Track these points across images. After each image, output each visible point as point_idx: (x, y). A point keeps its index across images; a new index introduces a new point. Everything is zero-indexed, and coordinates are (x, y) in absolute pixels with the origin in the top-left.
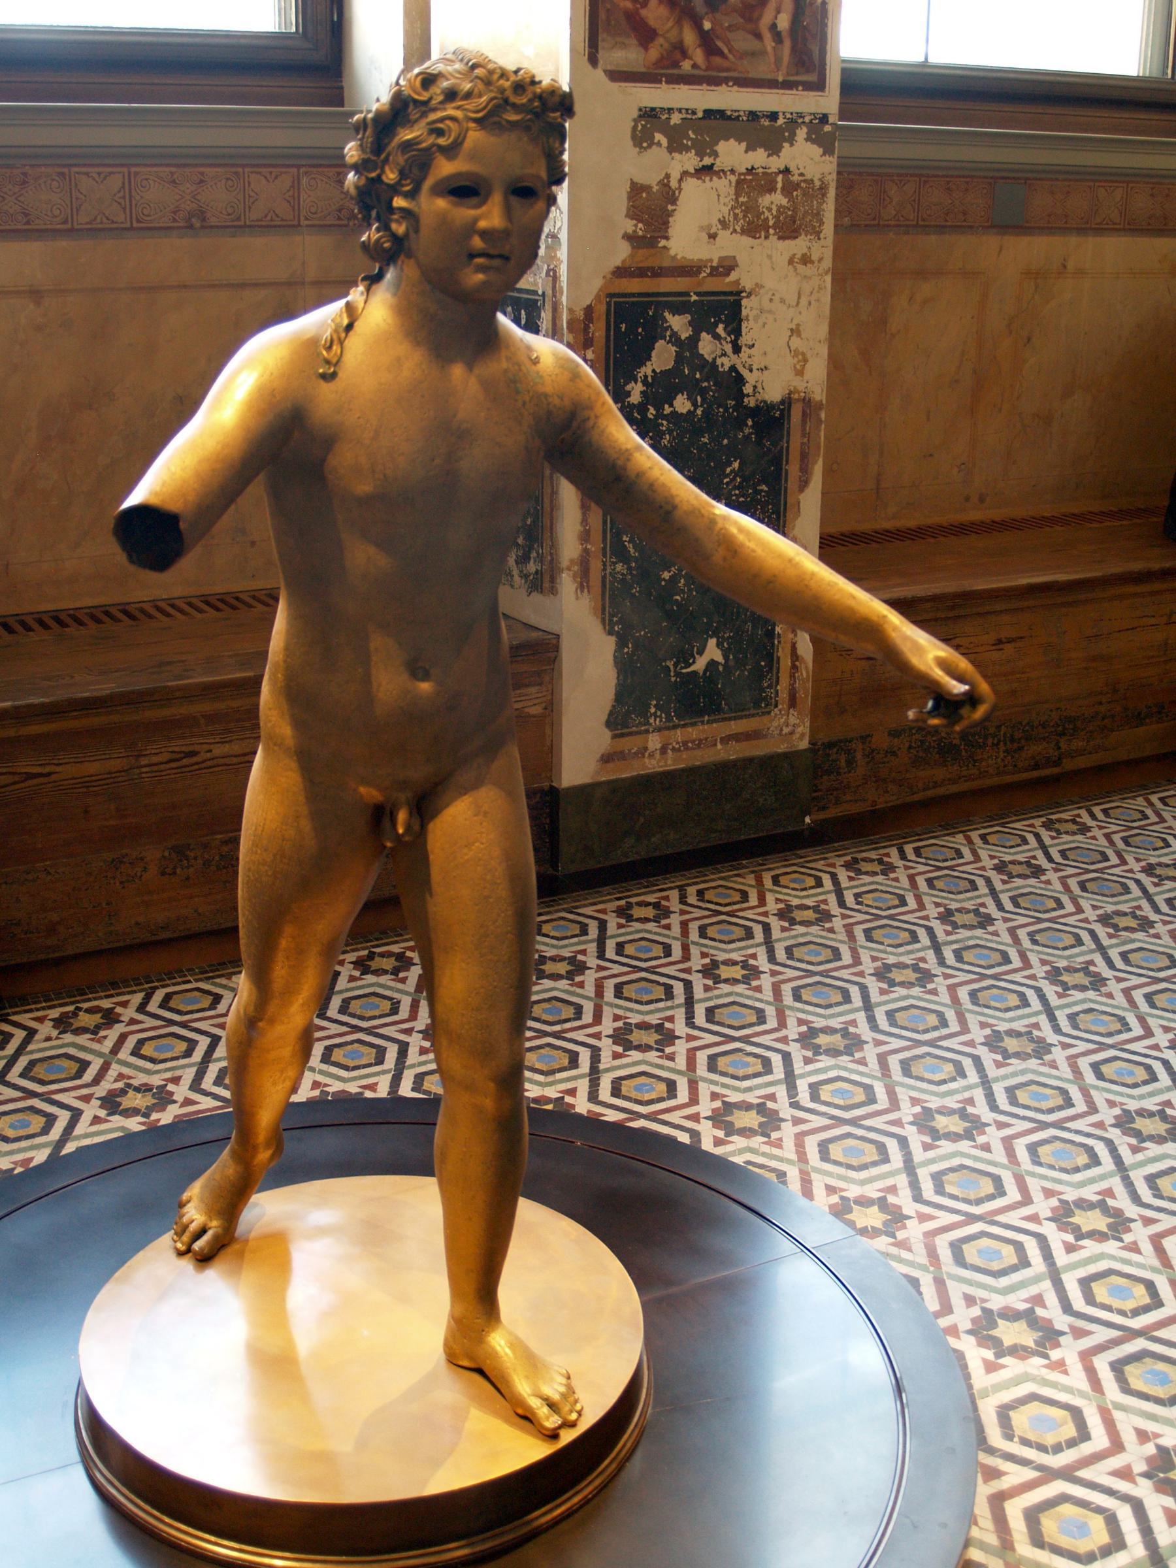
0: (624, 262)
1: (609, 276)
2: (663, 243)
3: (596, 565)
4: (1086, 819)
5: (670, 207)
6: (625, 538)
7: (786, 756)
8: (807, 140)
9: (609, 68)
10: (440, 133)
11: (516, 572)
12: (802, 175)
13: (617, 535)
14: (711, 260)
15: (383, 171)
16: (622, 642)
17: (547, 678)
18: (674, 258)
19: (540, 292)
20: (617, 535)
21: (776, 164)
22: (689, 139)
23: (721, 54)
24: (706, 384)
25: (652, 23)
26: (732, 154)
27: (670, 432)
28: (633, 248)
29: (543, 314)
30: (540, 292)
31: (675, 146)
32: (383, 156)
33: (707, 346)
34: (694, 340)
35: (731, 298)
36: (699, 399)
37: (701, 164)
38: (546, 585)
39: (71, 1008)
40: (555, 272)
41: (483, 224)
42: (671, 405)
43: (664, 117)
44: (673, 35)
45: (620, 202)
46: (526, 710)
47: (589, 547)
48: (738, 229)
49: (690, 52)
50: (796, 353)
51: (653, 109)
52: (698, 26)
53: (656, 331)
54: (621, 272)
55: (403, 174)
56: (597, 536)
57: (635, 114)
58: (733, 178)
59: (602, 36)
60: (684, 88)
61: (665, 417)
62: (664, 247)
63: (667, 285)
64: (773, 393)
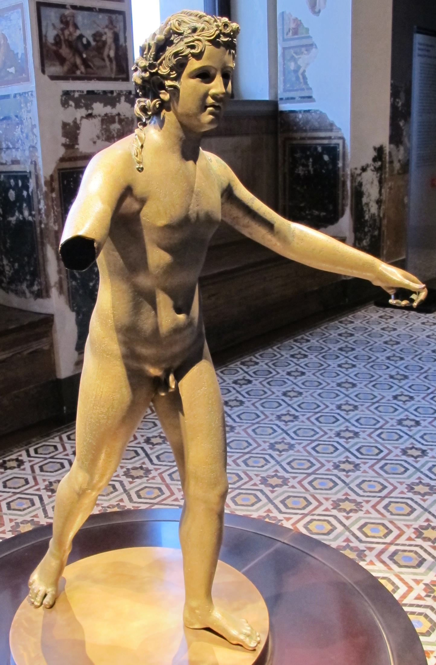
0: (63, 155)
4: (254, 359)
5: (78, 132)
8: (126, 101)
10: (193, 47)
11: (27, 291)
12: (124, 116)
15: (159, 69)
16: (78, 314)
18: (81, 153)
19: (28, 171)
21: (114, 111)
26: (99, 108)
30: (28, 171)
31: (78, 106)
32: (159, 62)
38: (44, 294)
41: (212, 91)
44: (72, 60)
45: (59, 131)
47: (61, 276)
48: (104, 139)
51: (68, 91)
54: (62, 160)
55: (172, 69)
57: (61, 93)
58: (100, 118)
59: (46, 61)
62: (77, 149)
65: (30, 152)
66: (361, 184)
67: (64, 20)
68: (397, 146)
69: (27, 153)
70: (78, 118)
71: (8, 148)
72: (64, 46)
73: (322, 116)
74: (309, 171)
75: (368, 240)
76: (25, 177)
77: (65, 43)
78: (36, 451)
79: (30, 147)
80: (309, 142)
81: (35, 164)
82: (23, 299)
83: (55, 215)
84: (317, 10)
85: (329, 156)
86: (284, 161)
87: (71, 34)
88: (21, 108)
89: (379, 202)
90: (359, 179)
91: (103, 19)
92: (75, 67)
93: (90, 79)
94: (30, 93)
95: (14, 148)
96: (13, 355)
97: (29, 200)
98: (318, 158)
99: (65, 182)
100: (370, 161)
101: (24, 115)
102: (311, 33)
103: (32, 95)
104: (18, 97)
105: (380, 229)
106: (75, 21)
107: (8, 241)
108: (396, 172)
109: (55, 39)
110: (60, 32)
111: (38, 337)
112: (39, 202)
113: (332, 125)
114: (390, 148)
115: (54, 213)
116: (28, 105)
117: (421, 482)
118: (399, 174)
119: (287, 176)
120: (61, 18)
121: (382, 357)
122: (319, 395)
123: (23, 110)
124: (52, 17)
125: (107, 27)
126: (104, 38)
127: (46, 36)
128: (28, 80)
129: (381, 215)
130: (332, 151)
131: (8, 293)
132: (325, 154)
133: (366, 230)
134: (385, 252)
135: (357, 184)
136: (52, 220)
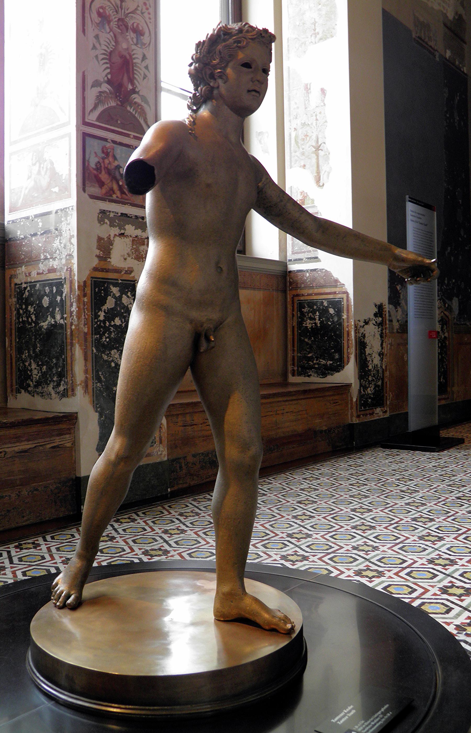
0: (96, 265)
1: (92, 270)
2: (109, 260)
3: (90, 383)
6: (100, 373)
7: (160, 463)
9: (90, 194)
13: (97, 372)
14: (125, 268)
16: (101, 415)
17: (72, 431)
19: (63, 278)
20: (97, 372)
22: (116, 223)
24: (125, 314)
25: (103, 179)
27: (114, 332)
28: (99, 260)
29: (65, 286)
30: (63, 278)
31: (112, 225)
33: (125, 300)
34: (121, 297)
35: (132, 283)
36: (123, 320)
37: (120, 233)
38: (70, 393)
40: (71, 268)
42: (114, 322)
43: (108, 214)
44: (110, 185)
45: (95, 244)
46: (65, 445)
48: (133, 257)
49: (116, 191)
51: (104, 210)
52: (118, 183)
53: (108, 293)
54: (95, 269)
57: (99, 211)
58: (131, 239)
59: (87, 182)
61: (112, 326)
63: (111, 276)
66: (364, 336)
67: (105, 151)
68: (396, 308)
71: (46, 259)
72: (103, 172)
73: (327, 274)
74: (315, 323)
75: (372, 389)
76: (59, 284)
77: (104, 170)
78: (53, 538)
79: (66, 256)
80: (315, 297)
82: (49, 400)
83: (85, 318)
84: (321, 184)
85: (334, 310)
86: (293, 315)
87: (110, 163)
88: (61, 222)
90: (362, 330)
94: (70, 208)
95: (51, 258)
96: (35, 447)
97: (62, 304)
98: (324, 311)
99: (97, 290)
100: (372, 317)
101: (64, 227)
102: (316, 204)
103: (72, 209)
104: (60, 213)
105: (383, 379)
106: (115, 154)
107: (38, 345)
108: (395, 331)
109: (96, 165)
110: (101, 161)
111: (61, 433)
112: (71, 305)
113: (336, 281)
114: (389, 308)
115: (84, 316)
116: (68, 218)
117: (441, 558)
118: (398, 332)
119: (296, 329)
120: (103, 148)
123: (63, 223)
124: (95, 147)
127: (88, 161)
128: (69, 196)
129: (384, 367)
130: (337, 305)
131: (33, 396)
132: (330, 308)
133: (370, 379)
134: (388, 403)
135: (360, 335)
136: (83, 322)
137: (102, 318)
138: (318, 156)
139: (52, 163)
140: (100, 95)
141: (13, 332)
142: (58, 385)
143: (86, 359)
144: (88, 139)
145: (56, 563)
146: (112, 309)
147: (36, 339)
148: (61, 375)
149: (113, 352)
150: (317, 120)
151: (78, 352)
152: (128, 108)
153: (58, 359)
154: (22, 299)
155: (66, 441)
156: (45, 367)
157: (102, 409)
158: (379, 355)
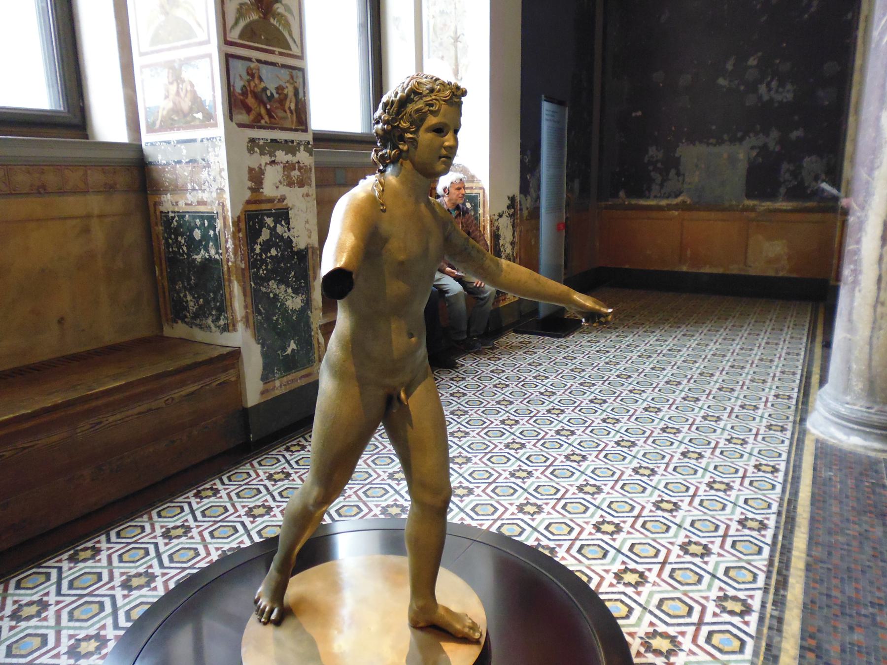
16: (263, 347)
21: (295, 159)
23: (273, 117)
26: (281, 156)
33: (279, 229)
34: (275, 227)
38: (231, 328)
39: (72, 552)
45: (246, 176)
50: (308, 230)
53: (262, 224)
54: (248, 202)
56: (250, 306)
59: (233, 109)
60: (262, 130)
63: (264, 206)
64: (302, 246)
65: (218, 194)
66: (498, 229)
68: (526, 196)
69: (214, 195)
70: (263, 164)
71: (194, 189)
72: (250, 95)
76: (212, 219)
81: (223, 206)
87: (256, 86)
88: (208, 152)
89: (512, 243)
91: (285, 74)
92: (259, 117)
93: (273, 128)
97: (216, 239)
100: (505, 209)
101: (211, 158)
104: (205, 141)
109: (242, 90)
111: (225, 370)
112: (227, 241)
113: (473, 177)
121: (530, 378)
122: (483, 412)
124: (239, 68)
125: (288, 81)
126: (285, 92)
128: (215, 125)
130: (473, 199)
137: (258, 251)
138: (456, 48)
139: (192, 85)
140: (241, 7)
141: (163, 261)
142: (218, 319)
143: (245, 295)
144: (231, 60)
145: (239, 516)
146: (267, 240)
147: (189, 271)
148: (221, 310)
149: (270, 283)
150: (455, 8)
151: (236, 288)
152: (272, 20)
153: (215, 293)
154: (170, 228)
155: (231, 376)
156: (201, 300)
157: (264, 340)
158: (511, 244)
